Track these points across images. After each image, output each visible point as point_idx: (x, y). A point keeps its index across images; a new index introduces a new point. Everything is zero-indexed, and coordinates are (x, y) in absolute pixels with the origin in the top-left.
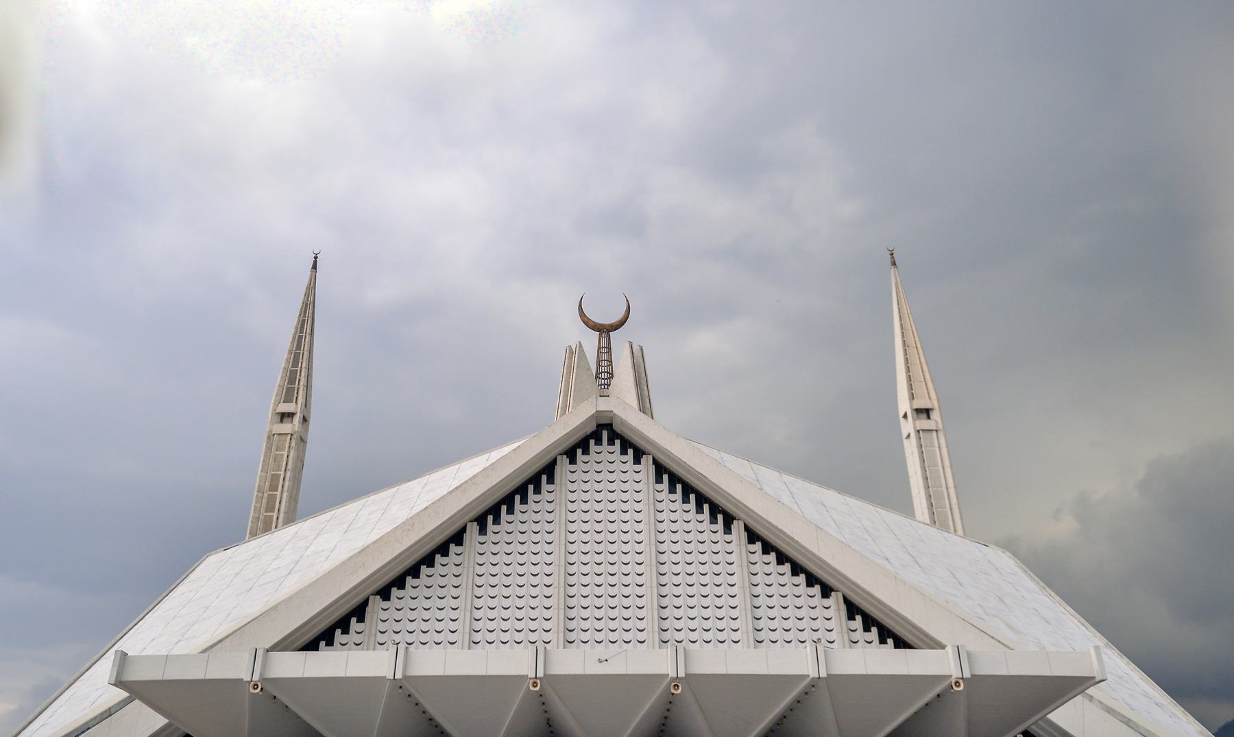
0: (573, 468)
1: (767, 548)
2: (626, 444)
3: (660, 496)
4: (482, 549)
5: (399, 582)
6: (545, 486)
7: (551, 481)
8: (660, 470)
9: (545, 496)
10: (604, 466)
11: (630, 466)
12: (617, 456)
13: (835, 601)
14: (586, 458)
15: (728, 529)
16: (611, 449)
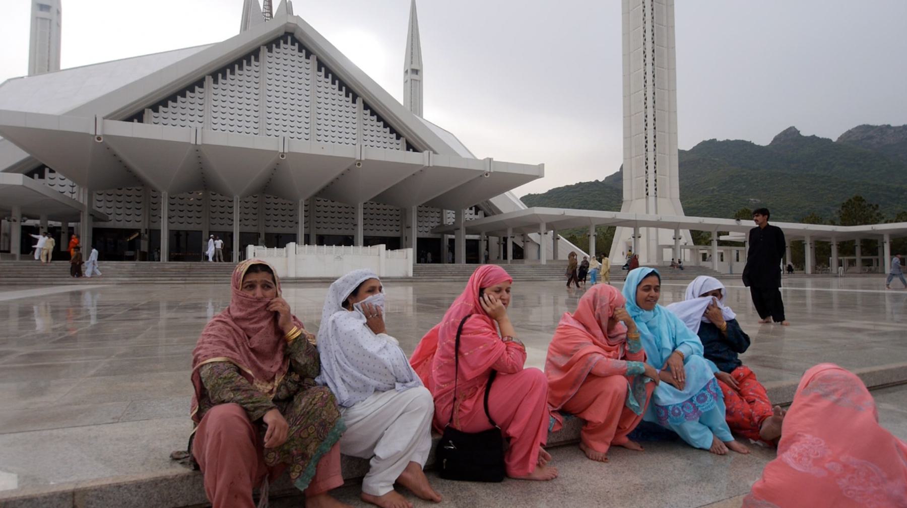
0: (270, 54)
1: (373, 113)
2: (302, 47)
3: (320, 79)
4: (215, 91)
5: (164, 103)
6: (253, 62)
7: (257, 59)
8: (321, 65)
9: (253, 68)
10: (289, 57)
11: (303, 59)
12: (296, 52)
13: (402, 142)
14: (278, 50)
15: (354, 102)
16: (293, 47)
